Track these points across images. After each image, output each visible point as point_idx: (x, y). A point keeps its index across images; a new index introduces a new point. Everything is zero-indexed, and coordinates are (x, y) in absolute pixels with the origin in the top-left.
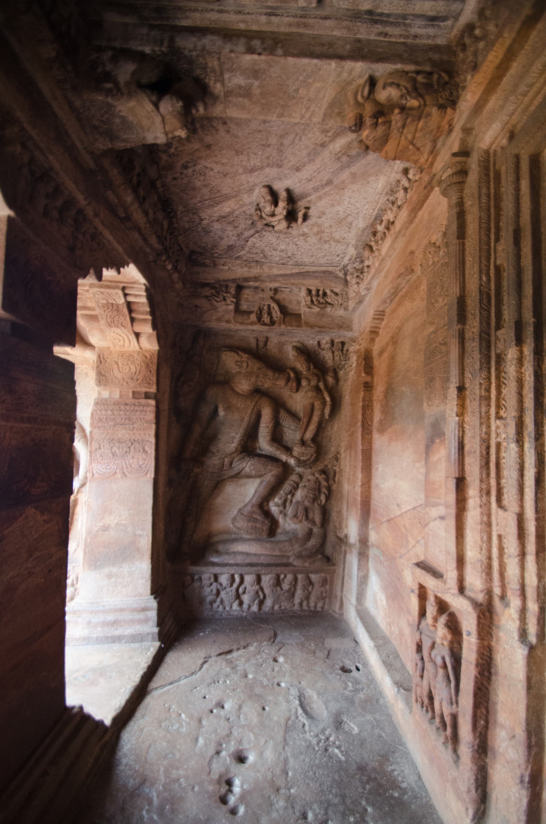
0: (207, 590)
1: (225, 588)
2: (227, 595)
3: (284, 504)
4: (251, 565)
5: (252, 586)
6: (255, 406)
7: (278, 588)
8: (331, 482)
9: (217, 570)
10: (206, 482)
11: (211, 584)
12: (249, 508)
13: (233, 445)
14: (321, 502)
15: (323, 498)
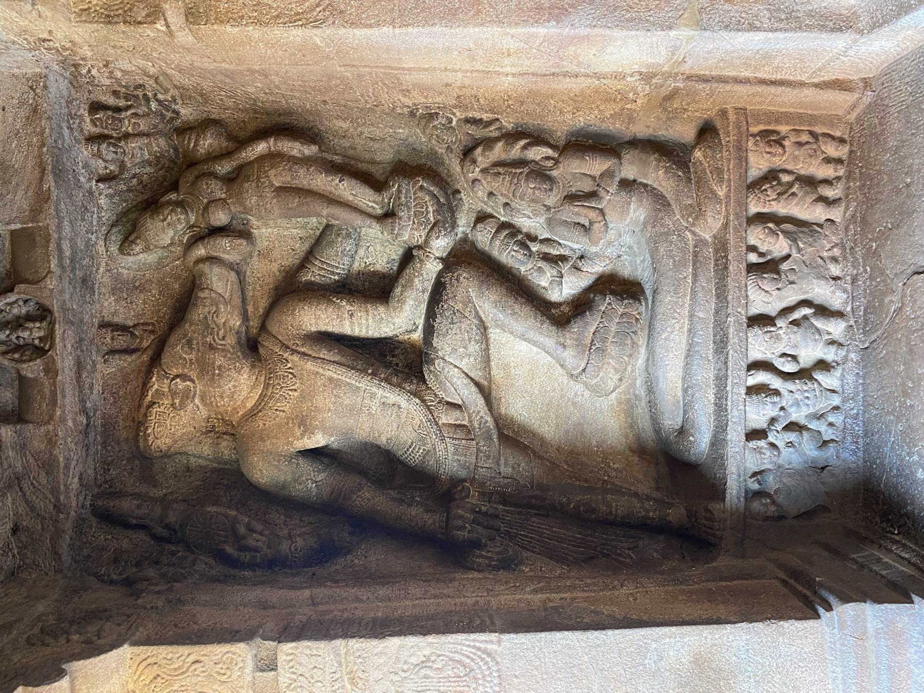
0: (787, 454)
1: (782, 408)
2: (798, 402)
3: (555, 260)
4: (721, 345)
5: (778, 338)
6: (294, 352)
7: (784, 266)
8: (492, 132)
9: (735, 435)
10: (506, 470)
11: (773, 445)
12: (569, 355)
13: (404, 404)
14: (548, 158)
15: (538, 153)
